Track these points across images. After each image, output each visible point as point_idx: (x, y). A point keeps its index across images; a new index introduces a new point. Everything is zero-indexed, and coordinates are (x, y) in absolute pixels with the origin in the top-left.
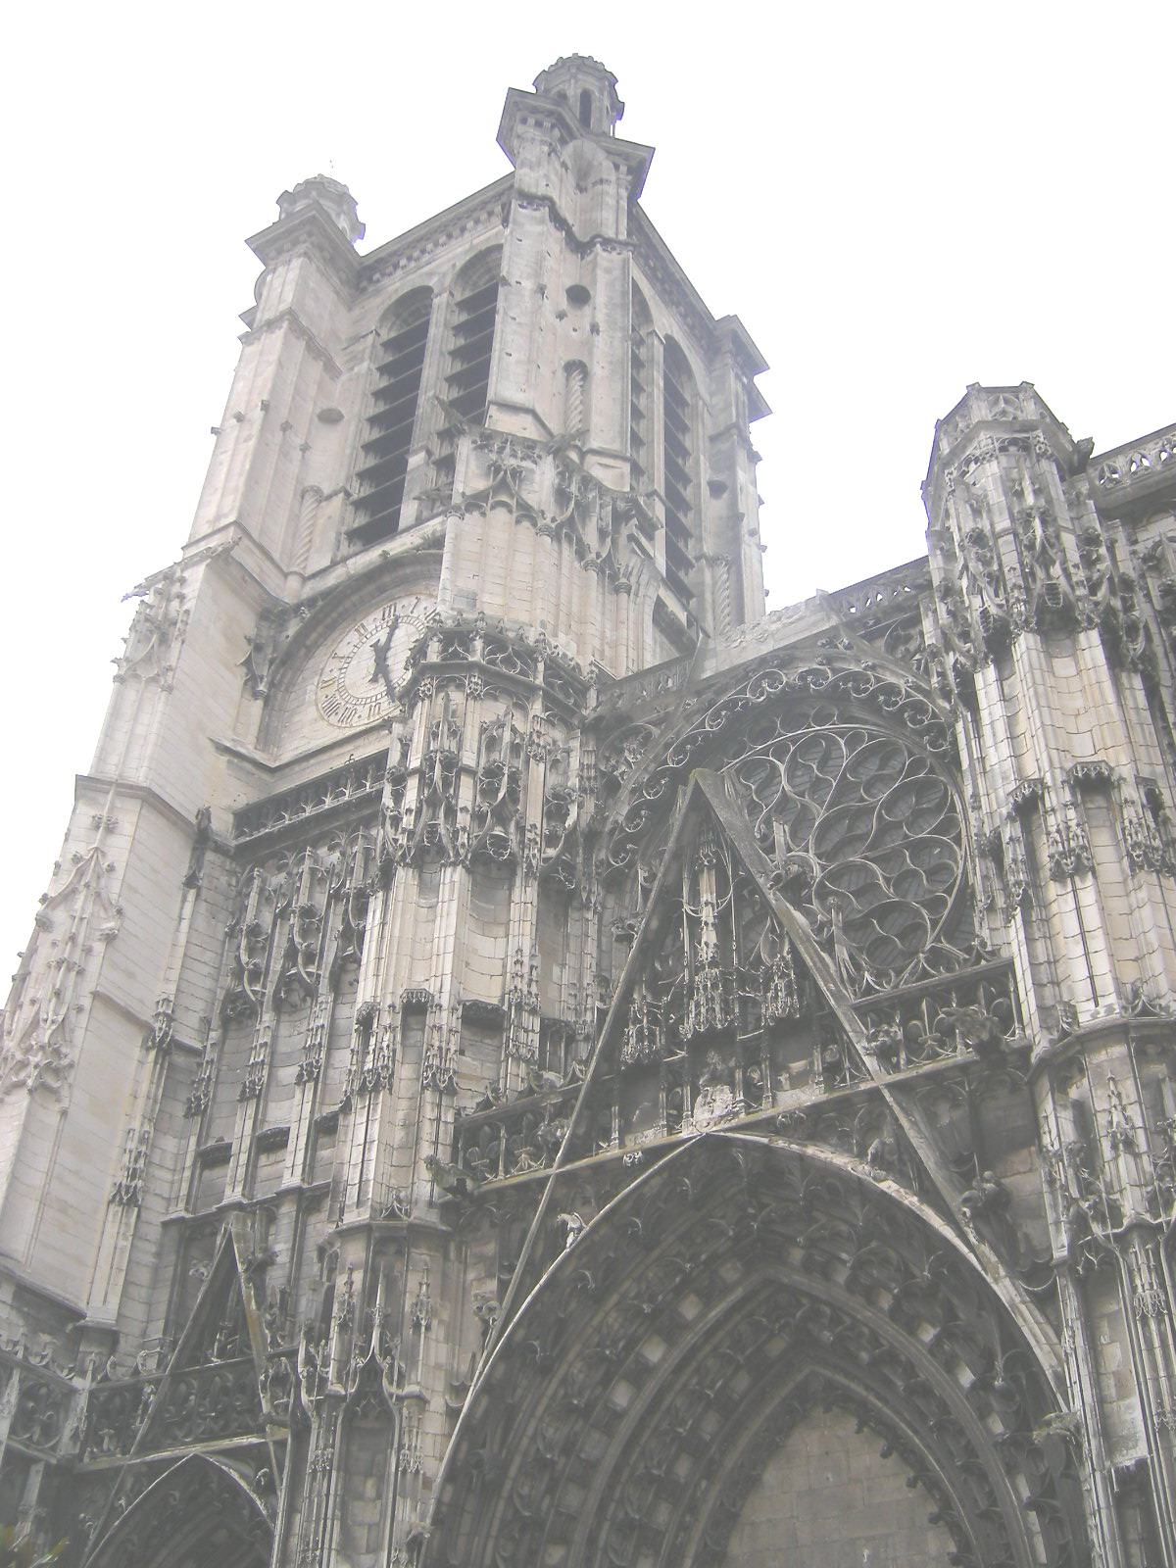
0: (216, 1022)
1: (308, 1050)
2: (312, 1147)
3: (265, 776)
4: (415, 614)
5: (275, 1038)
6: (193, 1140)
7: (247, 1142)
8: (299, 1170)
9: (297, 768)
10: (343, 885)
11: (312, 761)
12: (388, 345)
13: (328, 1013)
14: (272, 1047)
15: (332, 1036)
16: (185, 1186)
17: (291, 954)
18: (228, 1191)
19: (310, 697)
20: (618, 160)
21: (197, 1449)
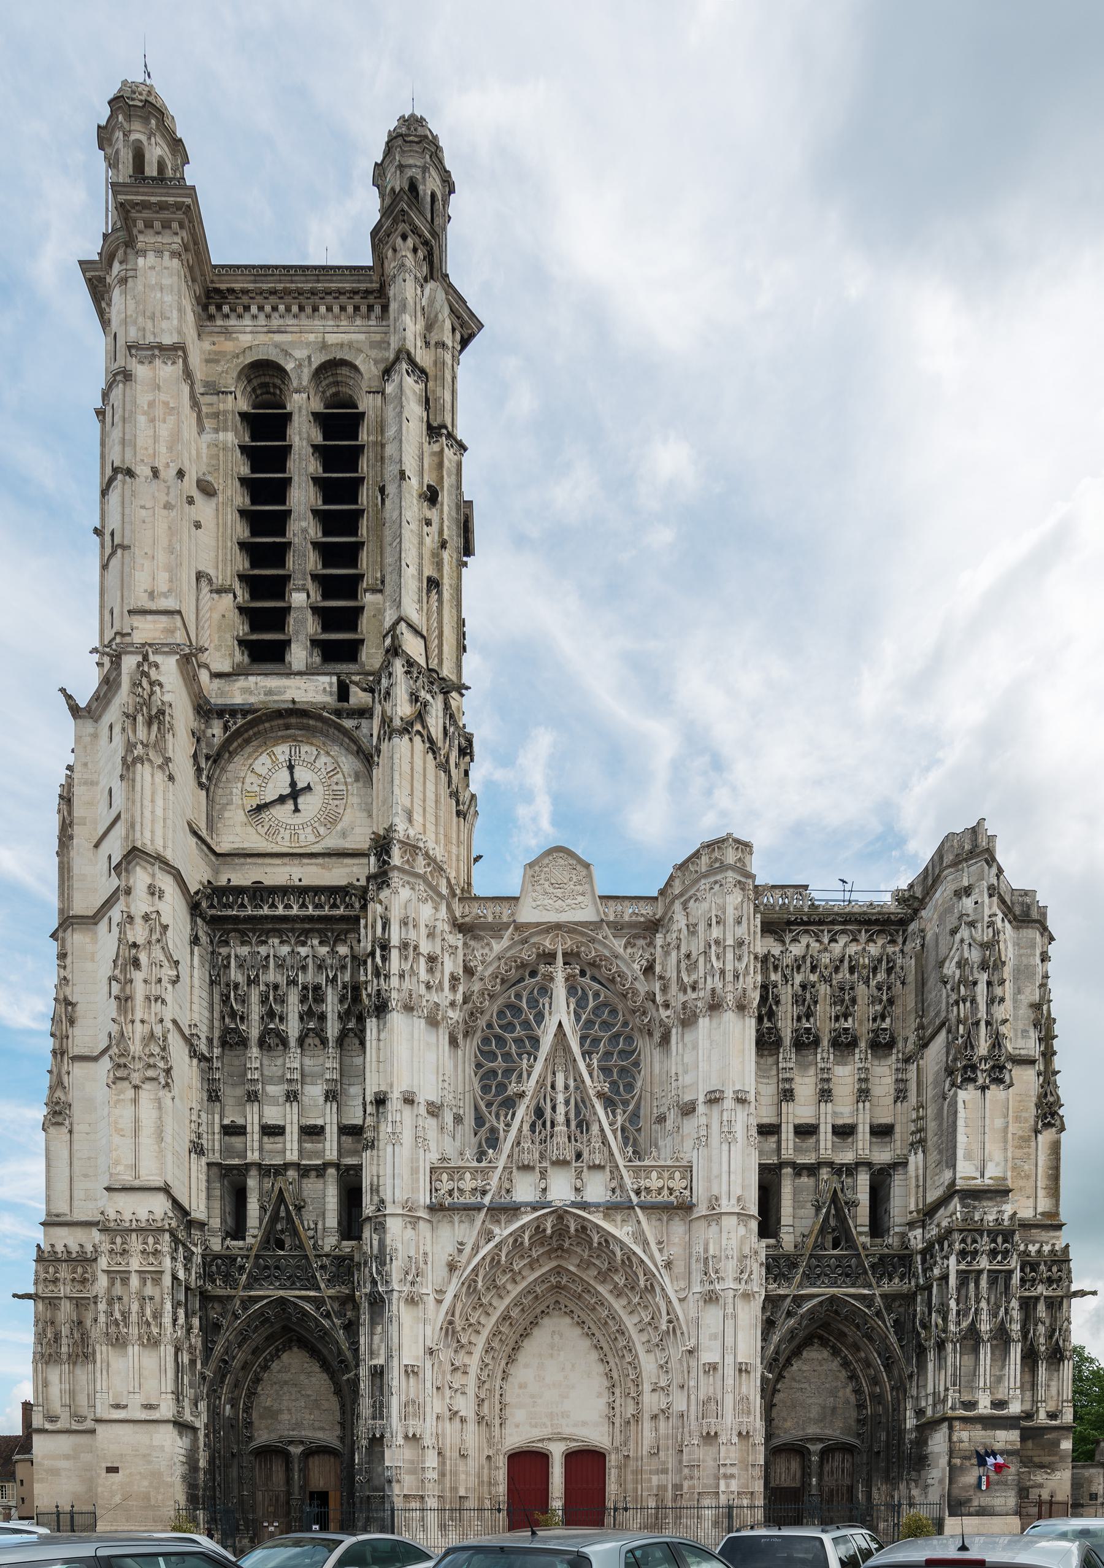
0: (216, 1042)
1: (290, 1081)
2: (300, 1141)
3: (213, 858)
4: (317, 764)
5: (261, 1065)
6: (217, 1117)
7: (257, 1128)
8: (296, 1153)
9: (237, 861)
10: (297, 975)
11: (249, 860)
12: (243, 416)
13: (298, 1060)
14: (260, 1069)
15: (302, 1075)
16: (217, 1144)
17: (271, 1014)
18: (249, 1153)
19: (236, 800)
20: (457, 326)
21: (281, 1293)
